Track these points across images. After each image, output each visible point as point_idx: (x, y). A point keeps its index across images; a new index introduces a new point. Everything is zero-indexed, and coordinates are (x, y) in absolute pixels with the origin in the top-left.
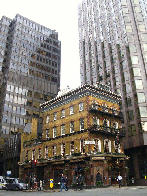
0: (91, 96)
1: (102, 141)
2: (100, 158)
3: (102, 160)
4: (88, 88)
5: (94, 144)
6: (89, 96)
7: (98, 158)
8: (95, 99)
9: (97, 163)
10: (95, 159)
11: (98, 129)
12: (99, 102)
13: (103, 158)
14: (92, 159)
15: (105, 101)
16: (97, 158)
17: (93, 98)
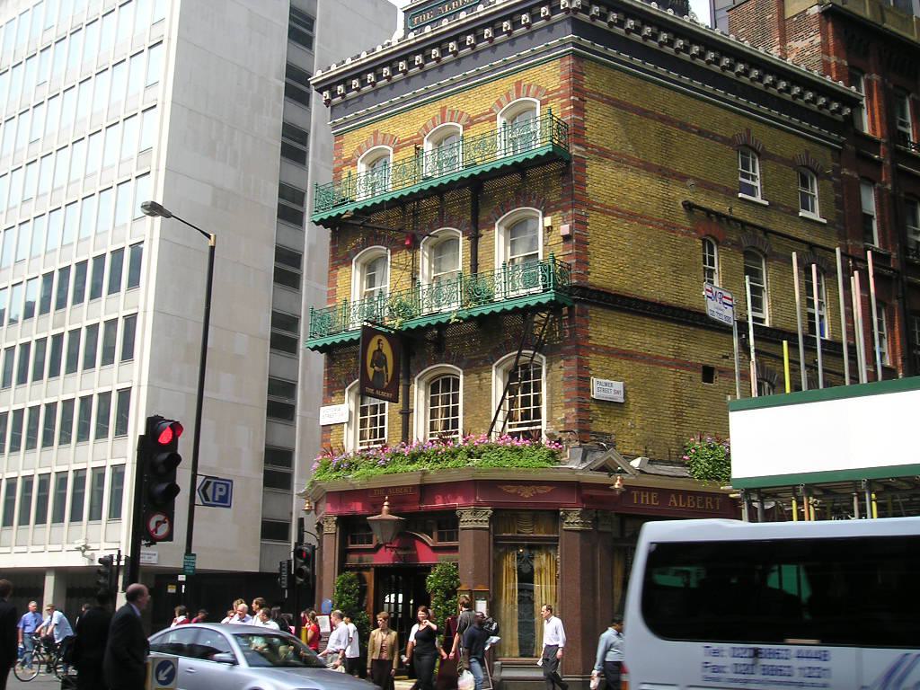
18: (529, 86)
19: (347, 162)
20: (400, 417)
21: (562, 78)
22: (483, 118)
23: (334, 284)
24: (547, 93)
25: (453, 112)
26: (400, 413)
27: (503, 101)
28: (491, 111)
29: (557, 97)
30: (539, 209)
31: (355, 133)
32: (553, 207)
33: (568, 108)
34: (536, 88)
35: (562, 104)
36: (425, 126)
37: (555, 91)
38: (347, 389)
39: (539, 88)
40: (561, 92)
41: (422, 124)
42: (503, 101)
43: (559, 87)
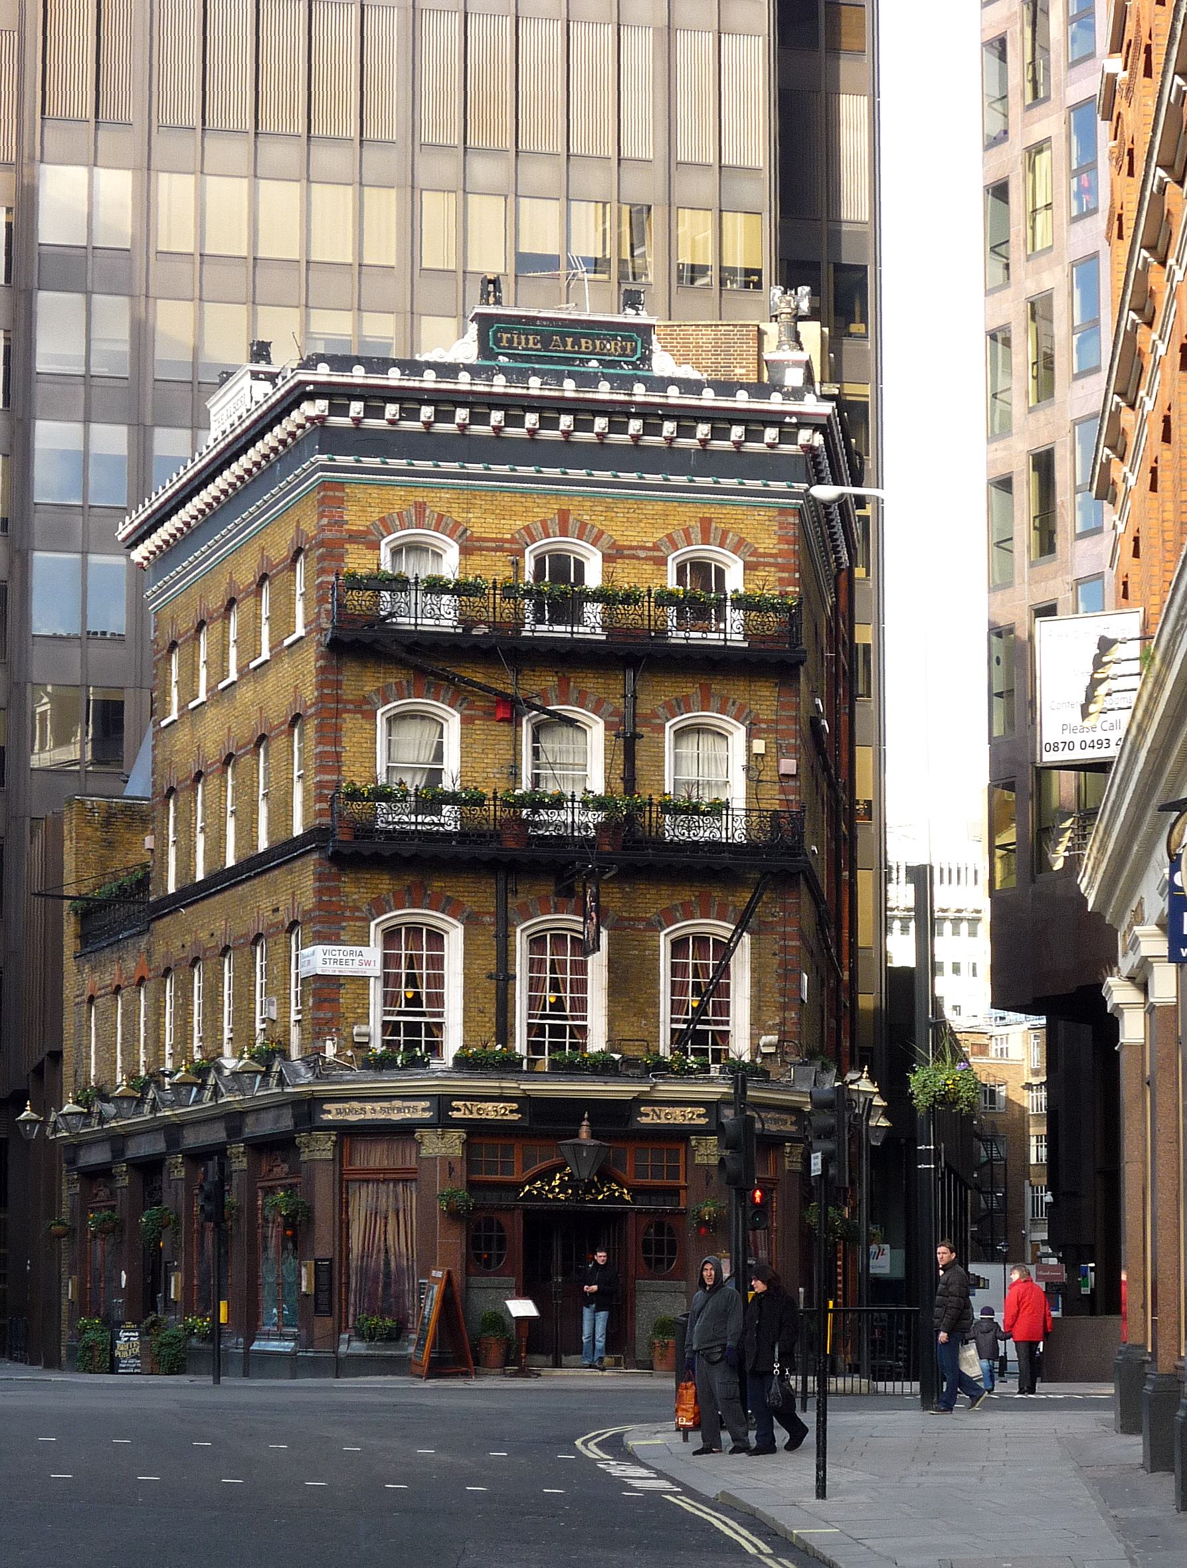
0: (359, 483)
1: (487, 938)
2: (398, 1113)
3: (405, 1131)
4: (321, 406)
5: (375, 969)
6: (340, 485)
7: (378, 1106)
8: (421, 507)
9: (375, 1156)
10: (352, 1118)
11: (448, 818)
12: (482, 524)
13: (420, 1111)
14: (332, 1113)
15: (582, 512)
16: (373, 1112)
17: (399, 499)
18: (725, 533)
19: (355, 537)
20: (491, 985)
21: (782, 539)
22: (642, 554)
23: (337, 741)
24: (755, 553)
25: (583, 525)
26: (490, 977)
27: (679, 537)
28: (656, 548)
29: (770, 565)
30: (742, 723)
31: (374, 492)
32: (764, 726)
33: (790, 589)
34: (736, 539)
35: (780, 579)
36: (527, 528)
37: (771, 555)
38: (373, 924)
39: (741, 541)
40: (780, 560)
41: (520, 524)
42: (679, 537)
43: (774, 551)
